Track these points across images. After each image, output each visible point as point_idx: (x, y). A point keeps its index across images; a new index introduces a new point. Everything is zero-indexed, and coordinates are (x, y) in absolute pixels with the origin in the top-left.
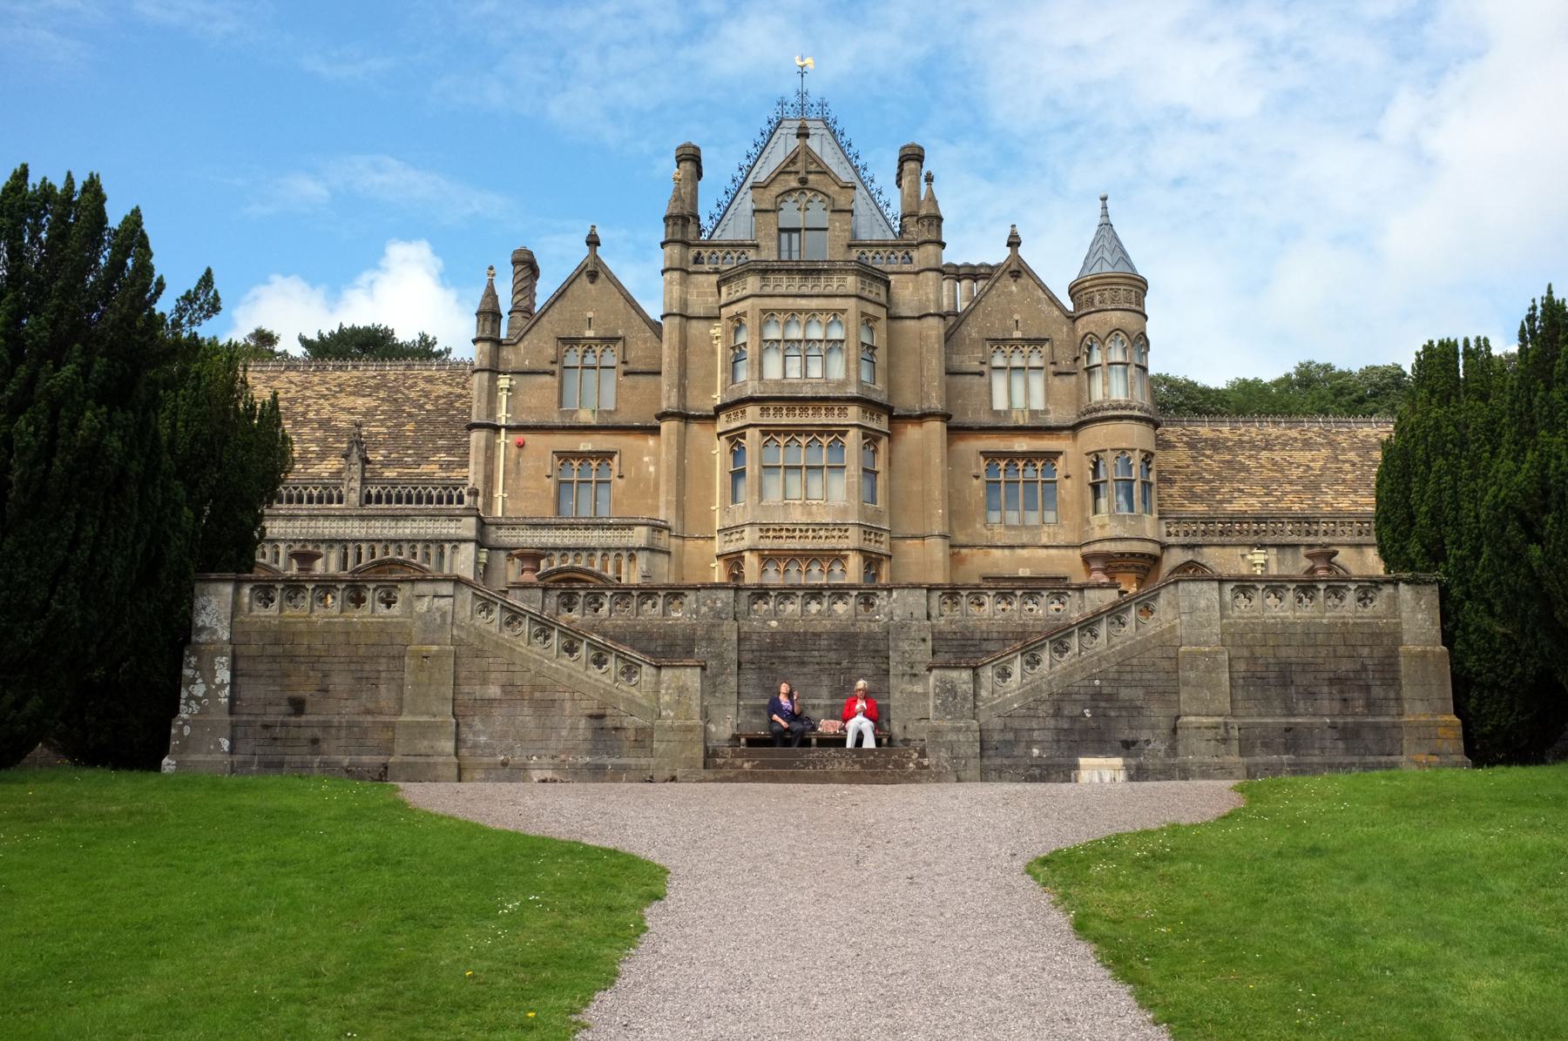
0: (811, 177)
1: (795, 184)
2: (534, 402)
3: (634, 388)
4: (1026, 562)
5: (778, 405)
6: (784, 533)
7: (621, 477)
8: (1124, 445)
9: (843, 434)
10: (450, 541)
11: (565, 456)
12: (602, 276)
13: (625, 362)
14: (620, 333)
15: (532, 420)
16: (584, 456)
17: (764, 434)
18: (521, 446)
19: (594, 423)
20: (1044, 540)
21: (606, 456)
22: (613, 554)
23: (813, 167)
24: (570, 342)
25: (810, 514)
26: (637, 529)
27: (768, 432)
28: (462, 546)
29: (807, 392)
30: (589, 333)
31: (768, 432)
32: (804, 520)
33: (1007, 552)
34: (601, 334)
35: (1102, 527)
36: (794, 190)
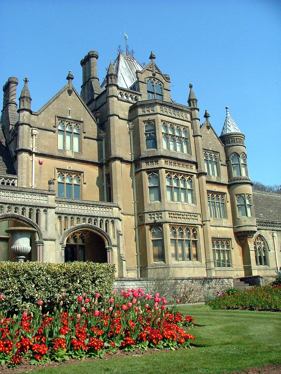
0: (156, 74)
1: (151, 75)
2: (47, 143)
3: (88, 144)
4: (220, 232)
5: (171, 161)
6: (177, 216)
7: (85, 184)
8: (249, 193)
9: (191, 176)
10: (43, 207)
11: (62, 171)
12: (74, 93)
13: (84, 133)
14: (82, 120)
15: (46, 152)
16: (70, 172)
17: (166, 172)
18: (41, 163)
19: (73, 157)
20: (224, 225)
21: (79, 173)
22: (105, 219)
23: (157, 71)
24: (62, 119)
25: (185, 208)
26: (114, 208)
27: (170, 172)
28: (49, 210)
29: (180, 157)
30: (70, 117)
31: (170, 172)
32: (183, 210)
33: (214, 228)
34: (74, 118)
35: (245, 221)
36: (152, 77)
